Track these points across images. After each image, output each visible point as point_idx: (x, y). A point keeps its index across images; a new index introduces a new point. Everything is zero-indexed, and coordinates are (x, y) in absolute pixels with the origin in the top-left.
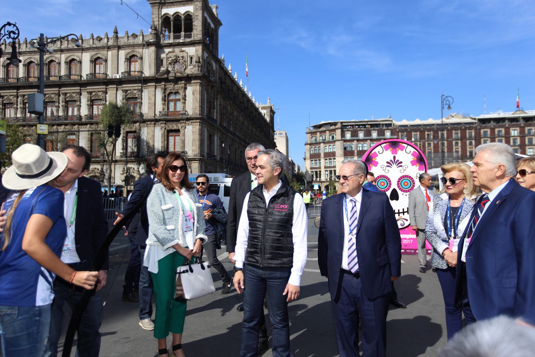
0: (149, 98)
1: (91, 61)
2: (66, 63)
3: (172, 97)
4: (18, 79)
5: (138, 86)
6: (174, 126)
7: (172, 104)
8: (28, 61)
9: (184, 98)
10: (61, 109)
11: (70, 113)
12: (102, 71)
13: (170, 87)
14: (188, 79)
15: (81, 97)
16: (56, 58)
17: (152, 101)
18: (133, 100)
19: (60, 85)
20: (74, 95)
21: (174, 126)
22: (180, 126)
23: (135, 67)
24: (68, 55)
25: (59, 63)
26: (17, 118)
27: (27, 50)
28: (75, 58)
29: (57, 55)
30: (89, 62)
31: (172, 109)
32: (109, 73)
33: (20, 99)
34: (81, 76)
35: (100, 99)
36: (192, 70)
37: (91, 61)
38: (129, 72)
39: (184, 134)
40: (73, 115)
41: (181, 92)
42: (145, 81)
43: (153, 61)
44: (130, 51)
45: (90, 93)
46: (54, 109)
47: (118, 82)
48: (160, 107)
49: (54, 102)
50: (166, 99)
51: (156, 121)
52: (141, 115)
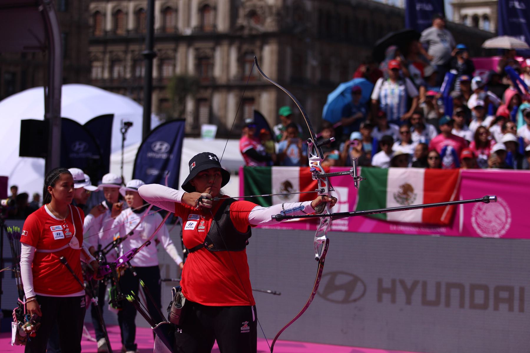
0: (223, 59)
3: (249, 57)
5: (211, 44)
6: (248, 94)
7: (248, 67)
9: (261, 59)
10: (128, 70)
11: (138, 74)
12: (173, 23)
13: (245, 47)
14: (265, 38)
17: (225, 63)
18: (204, 62)
21: (248, 94)
22: (255, 94)
23: (209, 17)
31: (247, 72)
32: (181, 25)
36: (269, 25)
38: (201, 27)
39: (259, 104)
40: (140, 77)
41: (257, 51)
42: (217, 38)
46: (122, 69)
47: (190, 40)
48: (234, 69)
50: (241, 61)
51: (228, 87)
52: (214, 79)
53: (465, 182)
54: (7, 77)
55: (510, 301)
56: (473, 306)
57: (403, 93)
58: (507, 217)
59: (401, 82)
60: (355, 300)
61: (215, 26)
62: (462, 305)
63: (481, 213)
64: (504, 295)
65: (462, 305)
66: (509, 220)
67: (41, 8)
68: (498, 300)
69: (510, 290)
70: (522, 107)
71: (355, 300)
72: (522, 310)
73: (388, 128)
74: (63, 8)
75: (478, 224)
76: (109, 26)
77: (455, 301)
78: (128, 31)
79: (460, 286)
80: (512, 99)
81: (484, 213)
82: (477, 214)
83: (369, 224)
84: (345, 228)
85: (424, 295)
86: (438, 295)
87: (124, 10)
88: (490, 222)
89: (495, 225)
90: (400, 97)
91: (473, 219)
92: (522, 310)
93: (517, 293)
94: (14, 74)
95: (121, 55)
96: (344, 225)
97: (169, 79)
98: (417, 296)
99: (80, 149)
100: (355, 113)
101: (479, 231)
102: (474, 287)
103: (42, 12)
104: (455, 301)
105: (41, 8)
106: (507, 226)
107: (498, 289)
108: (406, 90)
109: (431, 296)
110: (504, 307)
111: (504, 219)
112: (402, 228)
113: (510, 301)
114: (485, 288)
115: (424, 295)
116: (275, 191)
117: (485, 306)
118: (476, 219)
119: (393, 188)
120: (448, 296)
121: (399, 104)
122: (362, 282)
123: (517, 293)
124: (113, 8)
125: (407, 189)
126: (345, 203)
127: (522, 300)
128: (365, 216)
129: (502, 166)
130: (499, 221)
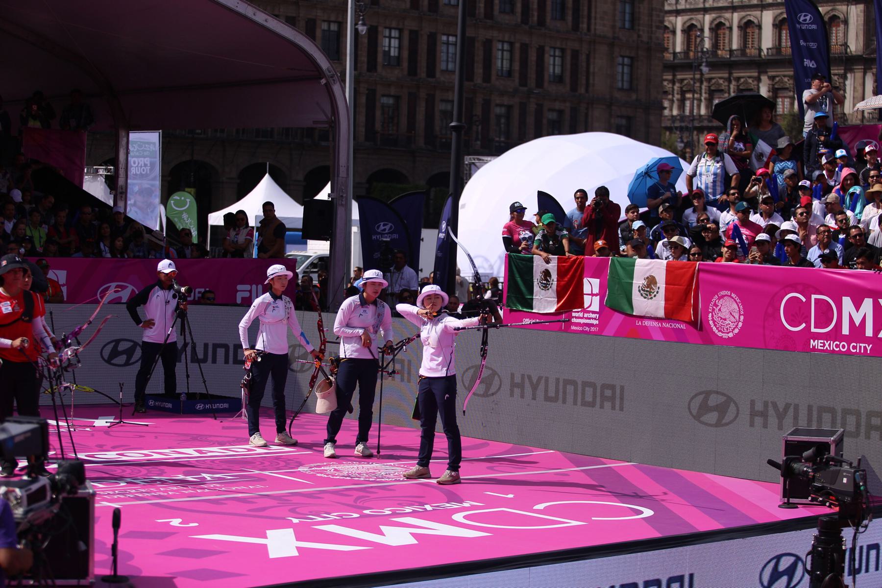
1: (774, 25)
2: (739, 27)
4: (675, 53)
8: (688, 24)
15: (761, 85)
16: (725, 19)
19: (729, 65)
20: (750, 81)
24: (743, 14)
25: (731, 28)
26: (672, 116)
27: (688, 7)
28: (752, 19)
29: (727, 15)
30: (771, 26)
33: (677, 87)
34: (760, 50)
35: (787, 89)
37: (774, 25)
43: (862, 27)
44: (829, 8)
45: (772, 78)
49: (722, 91)
53: (702, 275)
54: (553, 116)
55: (612, 399)
56: (585, 404)
57: (719, 171)
58: (740, 315)
59: (718, 159)
60: (493, 394)
61: (846, 45)
62: (575, 403)
63: (717, 310)
64: (608, 393)
65: (575, 403)
66: (742, 318)
67: (323, 81)
68: (604, 398)
69: (612, 387)
70: (851, 190)
71: (493, 394)
72: (621, 409)
73: (705, 209)
74: (627, 25)
75: (714, 322)
76: (707, 44)
77: (570, 398)
78: (731, 51)
79: (573, 383)
80: (845, 179)
81: (720, 310)
82: (713, 310)
83: (618, 318)
84: (596, 322)
85: (546, 391)
86: (557, 392)
87: (727, 24)
88: (725, 320)
89: (729, 323)
90: (715, 174)
91: (710, 315)
92: (621, 409)
93: (618, 391)
94: (560, 112)
95: (724, 84)
96: (595, 319)
97: (783, 116)
98: (540, 393)
99: (385, 230)
100: (663, 194)
101: (714, 329)
102: (585, 384)
103: (326, 84)
104: (570, 398)
105: (323, 81)
106: (740, 325)
107: (604, 387)
108: (724, 168)
109: (552, 394)
110: (607, 405)
111: (737, 317)
112: (647, 323)
113: (612, 399)
114: (593, 385)
115: (546, 391)
116: (535, 283)
117: (592, 404)
118: (712, 316)
119: (638, 282)
120: (565, 392)
121: (714, 182)
122: (499, 376)
123: (618, 391)
124: (711, 23)
125: (651, 281)
126: (596, 295)
127: (622, 399)
128: (616, 311)
129: (767, 258)
130: (733, 320)
